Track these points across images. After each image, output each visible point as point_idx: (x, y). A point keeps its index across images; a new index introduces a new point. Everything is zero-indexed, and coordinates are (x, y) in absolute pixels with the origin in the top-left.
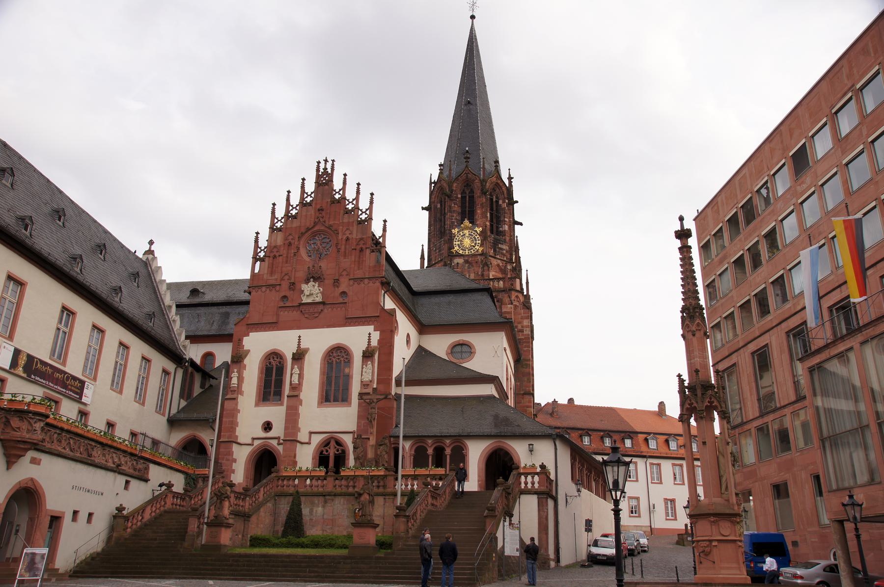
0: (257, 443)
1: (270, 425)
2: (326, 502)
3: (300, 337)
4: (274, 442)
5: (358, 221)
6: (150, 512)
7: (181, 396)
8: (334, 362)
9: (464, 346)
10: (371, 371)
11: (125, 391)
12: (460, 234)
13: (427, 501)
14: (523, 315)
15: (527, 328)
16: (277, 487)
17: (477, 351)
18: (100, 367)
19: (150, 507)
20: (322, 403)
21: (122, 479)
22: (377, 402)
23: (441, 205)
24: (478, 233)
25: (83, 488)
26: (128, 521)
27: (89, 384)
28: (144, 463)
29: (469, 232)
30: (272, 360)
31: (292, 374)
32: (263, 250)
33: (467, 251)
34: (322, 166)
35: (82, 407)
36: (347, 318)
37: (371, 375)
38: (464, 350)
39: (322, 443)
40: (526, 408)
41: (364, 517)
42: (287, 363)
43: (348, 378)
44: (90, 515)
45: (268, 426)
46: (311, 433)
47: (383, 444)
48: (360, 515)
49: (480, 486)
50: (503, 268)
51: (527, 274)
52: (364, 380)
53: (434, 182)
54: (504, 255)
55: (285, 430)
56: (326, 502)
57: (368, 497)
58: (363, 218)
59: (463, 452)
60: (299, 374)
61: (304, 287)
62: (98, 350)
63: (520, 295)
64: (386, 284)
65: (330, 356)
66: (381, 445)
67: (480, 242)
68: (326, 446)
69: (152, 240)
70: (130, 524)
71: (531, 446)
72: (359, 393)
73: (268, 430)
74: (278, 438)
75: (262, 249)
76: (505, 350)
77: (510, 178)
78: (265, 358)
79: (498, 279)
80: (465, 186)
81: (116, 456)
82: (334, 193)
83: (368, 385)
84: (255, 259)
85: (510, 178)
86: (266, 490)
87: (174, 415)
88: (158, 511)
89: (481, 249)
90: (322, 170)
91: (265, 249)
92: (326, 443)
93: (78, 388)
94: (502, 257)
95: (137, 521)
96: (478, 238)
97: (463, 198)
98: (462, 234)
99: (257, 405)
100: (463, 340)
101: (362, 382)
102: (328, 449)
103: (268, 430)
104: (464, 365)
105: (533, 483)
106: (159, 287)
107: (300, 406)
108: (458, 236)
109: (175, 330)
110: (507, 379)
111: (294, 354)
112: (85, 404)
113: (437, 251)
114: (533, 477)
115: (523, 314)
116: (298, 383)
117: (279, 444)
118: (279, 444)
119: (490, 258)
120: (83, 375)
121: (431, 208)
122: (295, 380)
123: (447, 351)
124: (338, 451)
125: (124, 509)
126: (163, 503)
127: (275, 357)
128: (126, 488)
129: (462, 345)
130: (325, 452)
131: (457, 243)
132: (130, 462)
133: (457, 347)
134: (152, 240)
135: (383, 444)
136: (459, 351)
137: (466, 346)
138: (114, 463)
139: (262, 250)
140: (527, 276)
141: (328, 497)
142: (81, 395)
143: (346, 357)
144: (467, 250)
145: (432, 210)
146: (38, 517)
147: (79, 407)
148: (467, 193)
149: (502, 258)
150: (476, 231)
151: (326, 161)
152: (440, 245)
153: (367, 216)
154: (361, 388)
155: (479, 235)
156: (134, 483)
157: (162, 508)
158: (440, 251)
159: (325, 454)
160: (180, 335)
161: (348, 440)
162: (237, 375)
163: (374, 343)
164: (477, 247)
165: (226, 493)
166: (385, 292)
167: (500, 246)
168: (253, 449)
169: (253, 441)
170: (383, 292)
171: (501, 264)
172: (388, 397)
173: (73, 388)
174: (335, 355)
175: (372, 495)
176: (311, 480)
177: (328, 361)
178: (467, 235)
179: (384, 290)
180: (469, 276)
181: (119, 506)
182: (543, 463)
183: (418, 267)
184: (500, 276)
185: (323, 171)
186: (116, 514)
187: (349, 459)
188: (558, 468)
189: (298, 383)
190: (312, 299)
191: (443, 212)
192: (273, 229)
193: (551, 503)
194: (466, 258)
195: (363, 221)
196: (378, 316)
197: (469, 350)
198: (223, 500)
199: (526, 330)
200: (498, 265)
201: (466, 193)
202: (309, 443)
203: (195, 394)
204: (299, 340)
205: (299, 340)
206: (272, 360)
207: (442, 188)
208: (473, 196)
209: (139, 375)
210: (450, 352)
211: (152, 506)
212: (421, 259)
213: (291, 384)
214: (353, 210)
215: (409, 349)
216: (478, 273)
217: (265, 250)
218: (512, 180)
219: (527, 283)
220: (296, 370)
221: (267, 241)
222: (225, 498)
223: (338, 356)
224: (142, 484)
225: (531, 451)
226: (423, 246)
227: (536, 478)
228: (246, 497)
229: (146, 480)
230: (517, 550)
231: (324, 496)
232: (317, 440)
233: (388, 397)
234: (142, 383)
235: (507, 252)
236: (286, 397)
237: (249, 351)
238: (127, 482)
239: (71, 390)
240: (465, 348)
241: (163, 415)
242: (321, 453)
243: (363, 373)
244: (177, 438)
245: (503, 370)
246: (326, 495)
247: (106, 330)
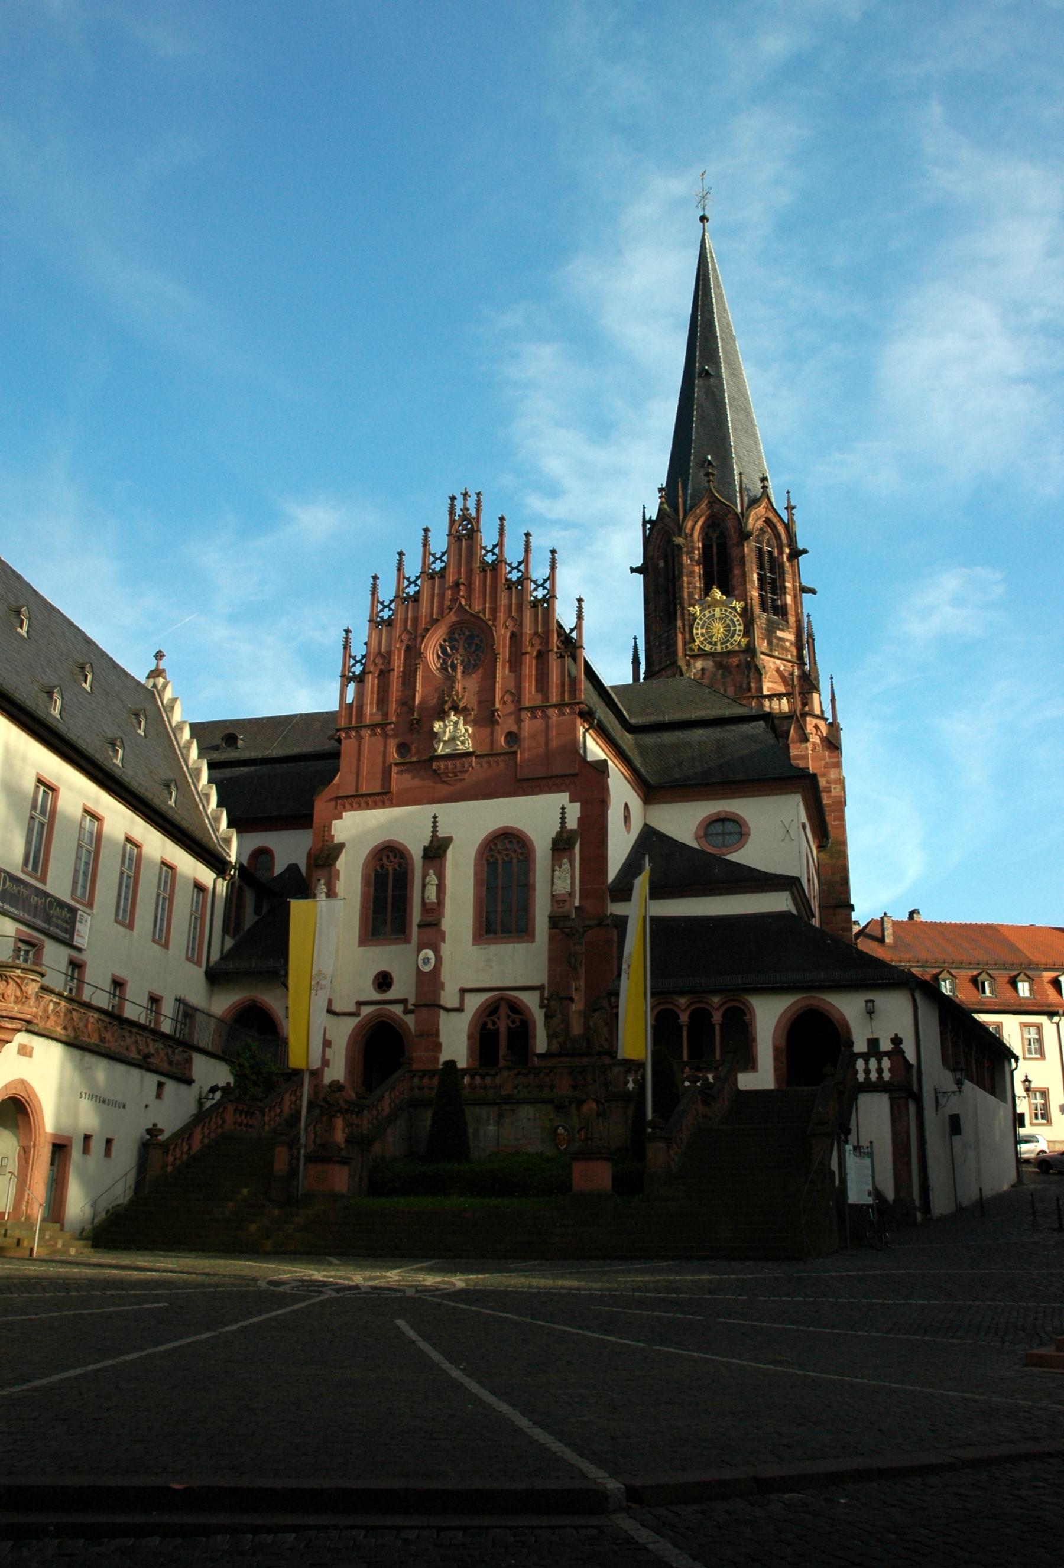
0: (366, 1010)
1: (389, 980)
2: (501, 1116)
3: (435, 817)
4: (398, 1009)
5: (531, 602)
6: (201, 1137)
7: (226, 930)
8: (500, 861)
9: (727, 823)
10: (569, 876)
11: (137, 924)
12: (704, 615)
13: (696, 1109)
14: (828, 760)
15: (836, 784)
16: (412, 1089)
17: (752, 832)
18: (98, 883)
19: (199, 1129)
20: (480, 936)
21: (152, 1080)
23: (666, 562)
24: (737, 612)
25: (96, 1096)
26: (167, 1154)
27: (83, 913)
28: (183, 1051)
29: (721, 610)
30: (385, 861)
31: (424, 886)
32: (360, 661)
33: (719, 647)
34: (459, 504)
35: (74, 953)
36: (518, 781)
37: (569, 882)
38: (728, 831)
39: (485, 1009)
40: (840, 932)
41: (589, 1142)
42: (412, 864)
43: (527, 888)
44: (109, 1141)
45: (384, 981)
46: (463, 991)
48: (583, 1137)
49: (777, 1079)
50: (786, 674)
51: (832, 684)
52: (558, 892)
53: (650, 521)
54: (787, 650)
55: (417, 987)
56: (501, 1116)
57: (594, 1106)
58: (540, 597)
59: (745, 1018)
60: (437, 885)
61: (437, 726)
62: (92, 854)
63: (822, 724)
64: (587, 715)
65: (491, 849)
66: (595, 1010)
67: (742, 628)
69: (159, 652)
70: (170, 1159)
71: (870, 1004)
72: (550, 917)
73: (385, 988)
74: (404, 1002)
75: (358, 659)
76: (804, 827)
77: (790, 508)
78: (374, 857)
79: (779, 696)
80: (709, 527)
81: (142, 1040)
82: (483, 552)
84: (346, 678)
85: (790, 508)
86: (393, 1096)
87: (216, 963)
88: (213, 1136)
89: (744, 641)
90: (458, 512)
91: (362, 659)
92: (491, 1010)
93: (67, 922)
94: (783, 654)
95: (182, 1154)
96: (738, 620)
97: (707, 548)
98: (708, 615)
99: (363, 942)
100: (726, 812)
101: (553, 896)
102: (496, 1020)
103: (385, 988)
104: (729, 857)
105: (880, 1071)
106: (178, 736)
107: (442, 944)
108: (701, 619)
109: (209, 812)
110: (809, 881)
111: (426, 849)
112: (79, 950)
113: (663, 647)
114: (879, 1062)
115: (830, 757)
116: (435, 901)
117: (406, 1012)
118: (406, 1012)
119: (762, 657)
120: (73, 899)
121: (647, 568)
122: (432, 894)
123: (696, 834)
124: (514, 1022)
125: (161, 1131)
126: (220, 1122)
127: (390, 854)
128: (159, 1096)
130: (490, 1026)
131: (699, 632)
132: (162, 1049)
133: (715, 824)
134: (159, 652)
136: (719, 831)
137: (731, 823)
138: (139, 1052)
139: (357, 662)
140: (832, 687)
141: (504, 1107)
142: (71, 931)
143: (520, 851)
144: (719, 644)
145: (650, 570)
146: (34, 1146)
147: (69, 955)
148: (714, 539)
149: (785, 657)
150: (734, 608)
151: (465, 495)
152: (668, 636)
153: (545, 592)
154: (552, 906)
155: (740, 615)
156: (170, 1086)
157: (220, 1131)
158: (667, 649)
159: (490, 1030)
160: (217, 819)
161: (531, 1001)
162: (325, 890)
163: (572, 824)
164: (736, 637)
165: (338, 1104)
166: (587, 730)
167: (779, 633)
168: (360, 1022)
169: (359, 1009)
170: (582, 730)
171: (782, 668)
172: (605, 923)
173: (59, 922)
174: (500, 847)
175: (602, 1103)
176: (472, 1077)
177: (488, 860)
178: (718, 615)
179: (584, 727)
180: (725, 690)
181: (150, 1126)
182: (896, 1035)
183: (630, 681)
184: (782, 689)
185: (461, 513)
186: (147, 1140)
187: (534, 1037)
188: (922, 1042)
189: (435, 901)
190: (453, 748)
191: (671, 575)
192: (375, 622)
193: (912, 1107)
194: (718, 659)
195: (539, 601)
196: (576, 775)
197: (737, 829)
198: (334, 1116)
199: (835, 788)
200: (778, 670)
201: (711, 539)
202: (460, 1009)
203: (247, 926)
204: (435, 822)
205: (435, 822)
206: (385, 861)
207: (666, 531)
208: (726, 543)
209: (158, 895)
210: (702, 833)
211: (203, 1127)
212: (633, 663)
213: (423, 903)
214: (520, 581)
215: (628, 831)
216: (741, 686)
217: (363, 661)
218: (793, 512)
219: (833, 700)
220: (433, 879)
221: (366, 644)
222: (337, 1111)
223: (507, 849)
224: (183, 1087)
225: (870, 1013)
226: (635, 638)
227: (886, 1063)
228: (363, 1110)
229: (189, 1082)
230: (870, 1194)
231: (499, 1104)
232: (474, 1002)
233: (605, 923)
234: (163, 909)
235: (791, 644)
236: (415, 929)
237: (341, 846)
238: (160, 1085)
239: (57, 926)
240: (730, 827)
241: (198, 963)
242: (484, 1025)
243: (555, 880)
244: (222, 1004)
245: (801, 865)
246: (502, 1103)
247: (104, 818)
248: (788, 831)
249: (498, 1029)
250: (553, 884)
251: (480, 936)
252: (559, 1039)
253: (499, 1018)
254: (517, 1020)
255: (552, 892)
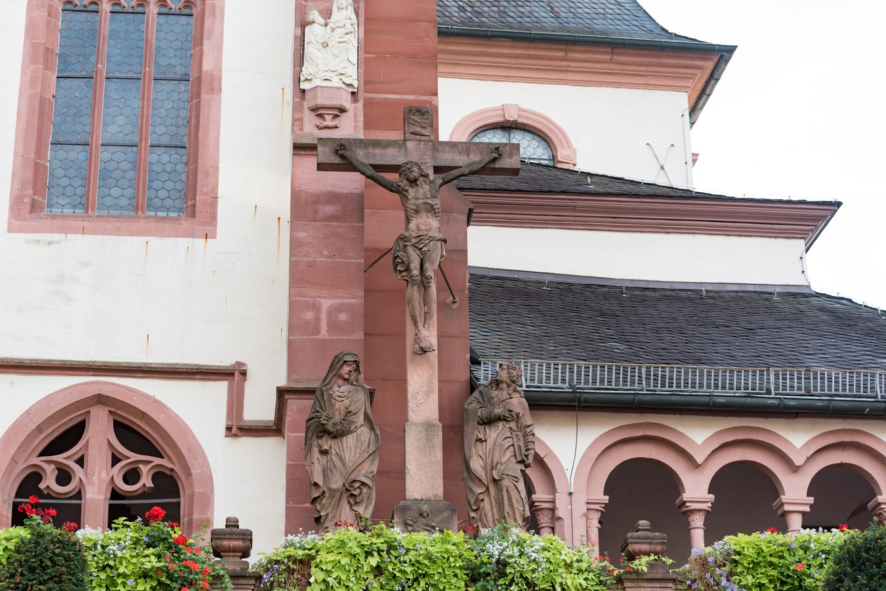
22: (441, 185)
39: (39, 429)
47: (499, 419)
52: (317, 82)
68: (50, 450)
83: (342, 110)
124: (131, 476)
129: (507, 127)
130: (49, 482)
135: (499, 419)
154: (297, 122)
243: (309, 50)
248: (662, 168)
249: (79, 495)
250: (300, 59)
251: (34, 207)
252: (360, 509)
253: (81, 462)
254: (144, 469)
255: (297, 80)
